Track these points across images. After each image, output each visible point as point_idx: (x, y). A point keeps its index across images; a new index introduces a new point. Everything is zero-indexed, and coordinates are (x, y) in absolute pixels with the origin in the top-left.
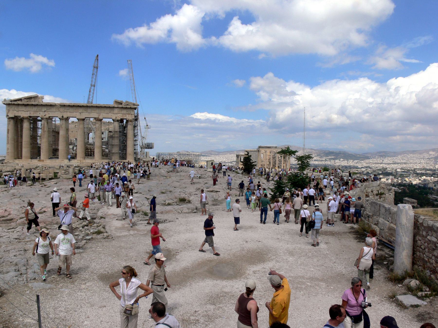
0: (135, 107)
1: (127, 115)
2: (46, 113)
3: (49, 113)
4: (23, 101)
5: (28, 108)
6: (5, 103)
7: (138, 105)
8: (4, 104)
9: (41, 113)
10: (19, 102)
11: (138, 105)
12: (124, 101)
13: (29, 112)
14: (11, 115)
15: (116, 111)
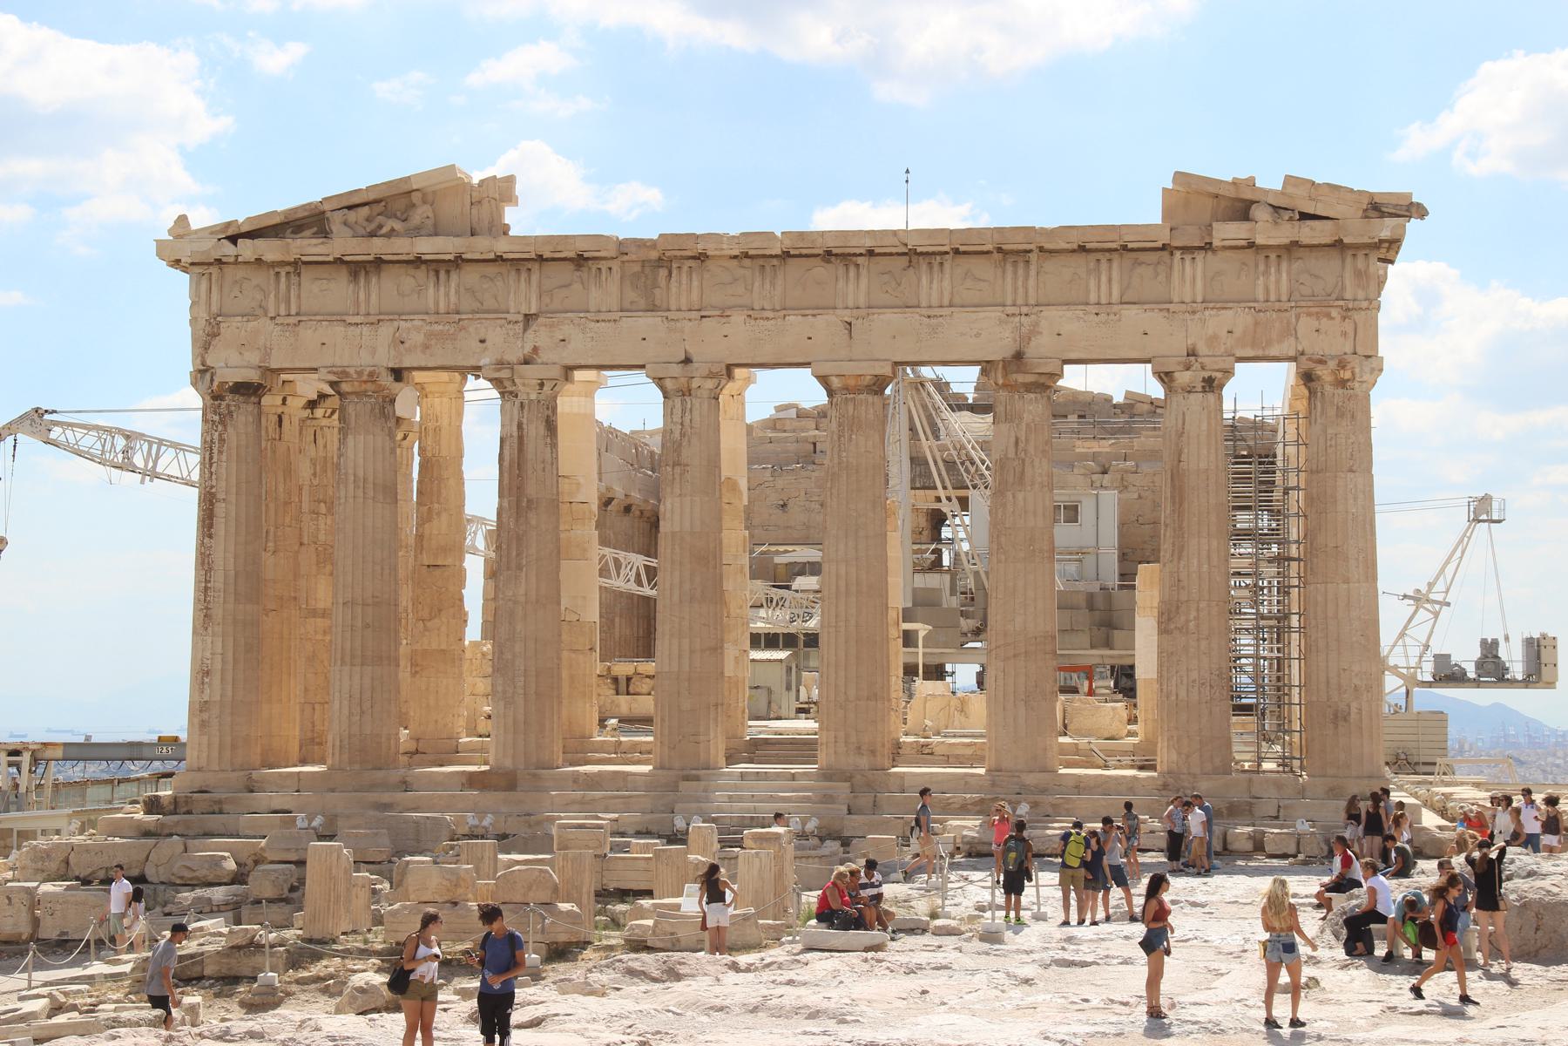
0: (1385, 229)
1: (1306, 325)
2: (539, 336)
3: (567, 330)
4: (336, 226)
5: (384, 290)
6: (186, 253)
7: (1420, 211)
8: (176, 263)
9: (496, 335)
10: (307, 246)
11: (1414, 210)
12: (1269, 180)
13: (386, 331)
14: (234, 366)
15: (1190, 277)
